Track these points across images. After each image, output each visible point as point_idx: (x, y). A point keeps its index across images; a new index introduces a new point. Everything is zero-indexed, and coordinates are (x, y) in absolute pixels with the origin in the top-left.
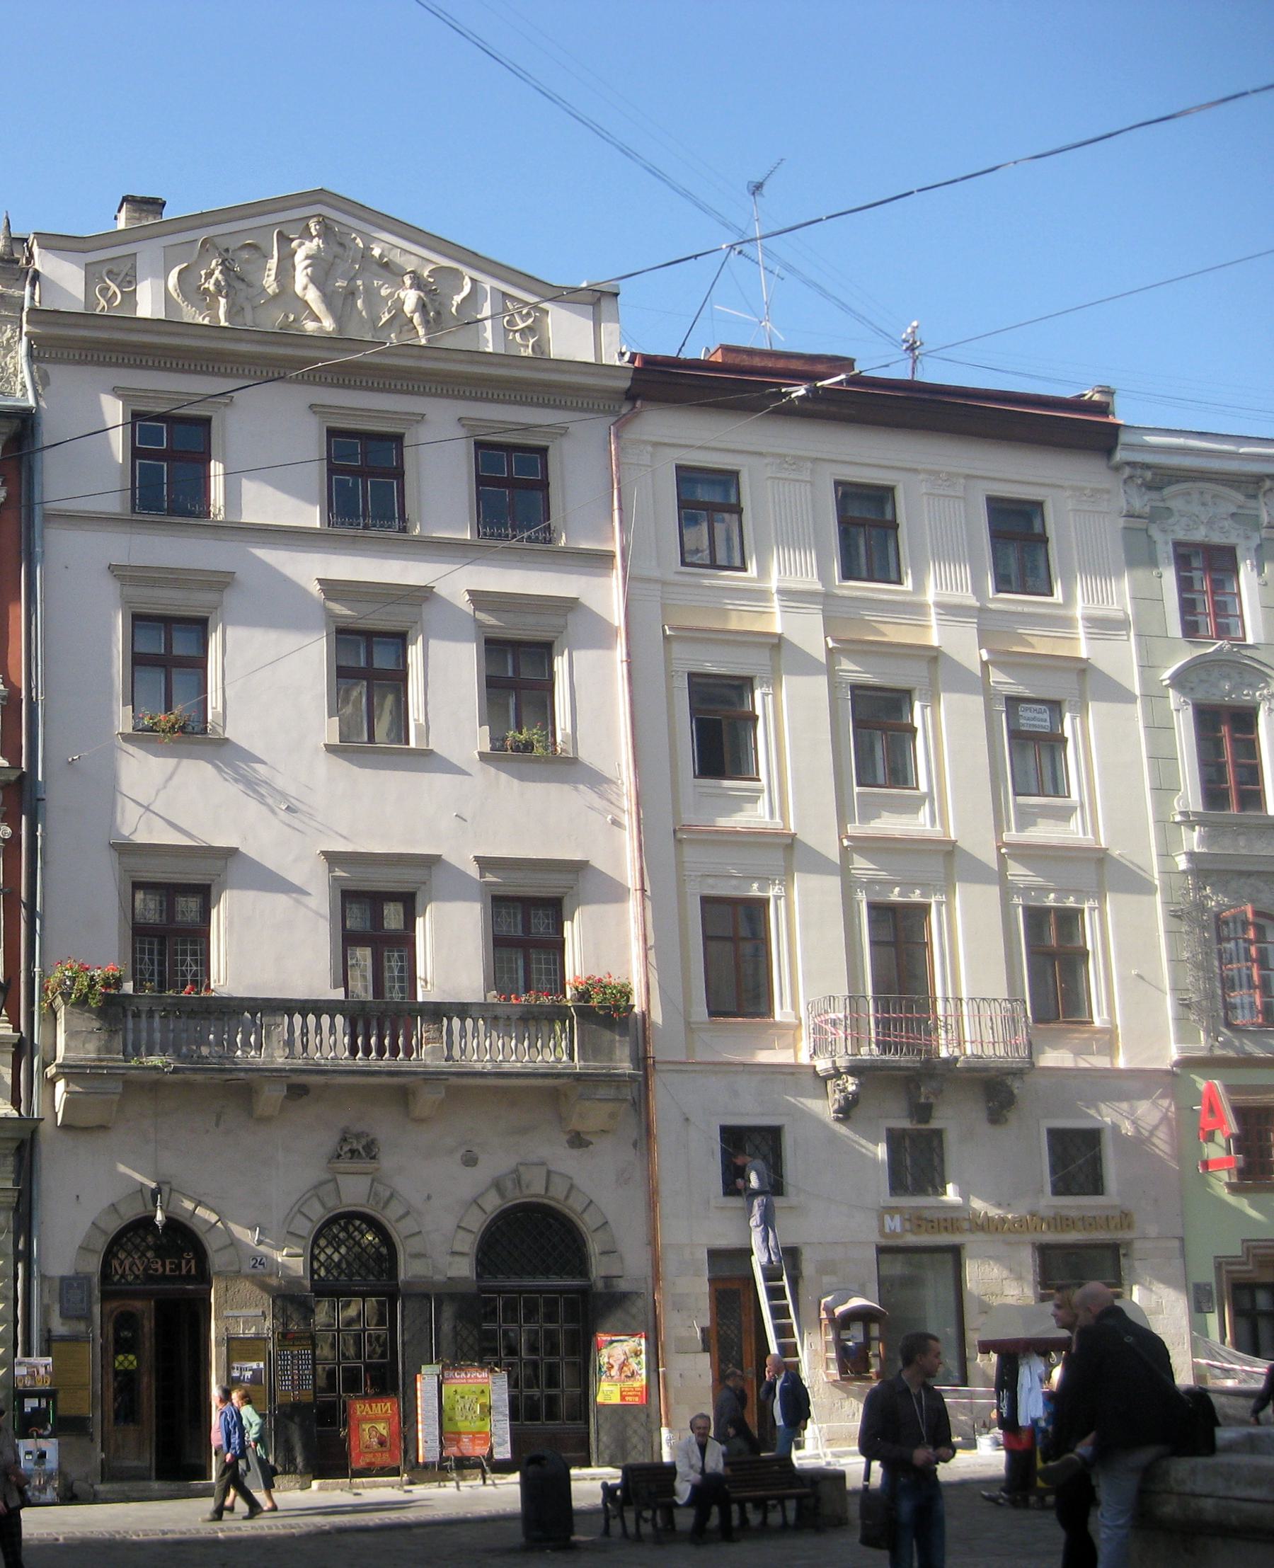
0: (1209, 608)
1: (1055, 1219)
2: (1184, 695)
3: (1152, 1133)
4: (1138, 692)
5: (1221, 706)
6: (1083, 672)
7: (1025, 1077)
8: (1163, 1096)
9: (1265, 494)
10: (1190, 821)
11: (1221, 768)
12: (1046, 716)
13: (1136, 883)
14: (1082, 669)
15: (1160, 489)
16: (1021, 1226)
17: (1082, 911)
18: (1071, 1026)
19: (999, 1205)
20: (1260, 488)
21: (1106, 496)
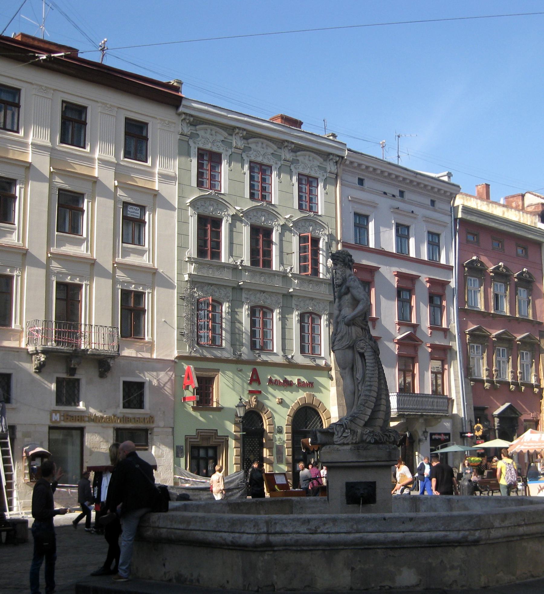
0: (208, 177)
1: (123, 418)
2: (194, 210)
3: (164, 385)
4: (176, 207)
5: (208, 217)
6: (155, 195)
7: (115, 359)
8: (169, 371)
9: (235, 135)
10: (191, 261)
11: (205, 242)
12: (139, 212)
13: (167, 284)
14: (155, 194)
15: (195, 126)
16: (109, 420)
17: (145, 293)
18: (138, 340)
19: (101, 411)
20: (234, 132)
21: (173, 125)
